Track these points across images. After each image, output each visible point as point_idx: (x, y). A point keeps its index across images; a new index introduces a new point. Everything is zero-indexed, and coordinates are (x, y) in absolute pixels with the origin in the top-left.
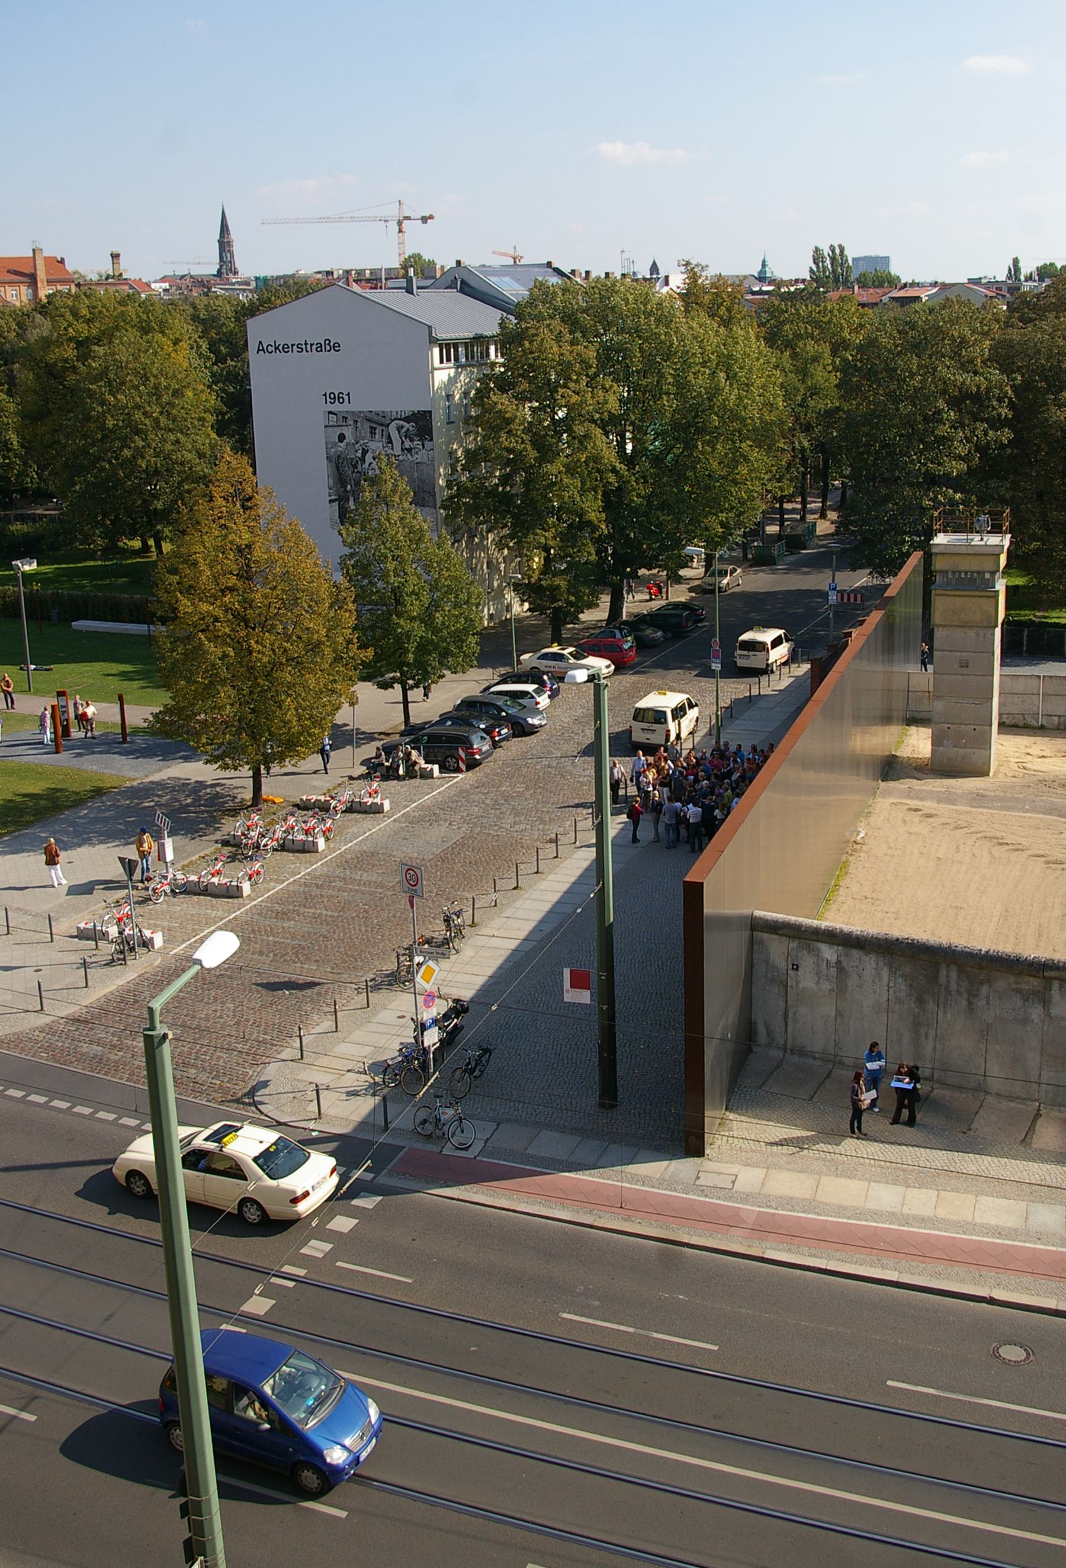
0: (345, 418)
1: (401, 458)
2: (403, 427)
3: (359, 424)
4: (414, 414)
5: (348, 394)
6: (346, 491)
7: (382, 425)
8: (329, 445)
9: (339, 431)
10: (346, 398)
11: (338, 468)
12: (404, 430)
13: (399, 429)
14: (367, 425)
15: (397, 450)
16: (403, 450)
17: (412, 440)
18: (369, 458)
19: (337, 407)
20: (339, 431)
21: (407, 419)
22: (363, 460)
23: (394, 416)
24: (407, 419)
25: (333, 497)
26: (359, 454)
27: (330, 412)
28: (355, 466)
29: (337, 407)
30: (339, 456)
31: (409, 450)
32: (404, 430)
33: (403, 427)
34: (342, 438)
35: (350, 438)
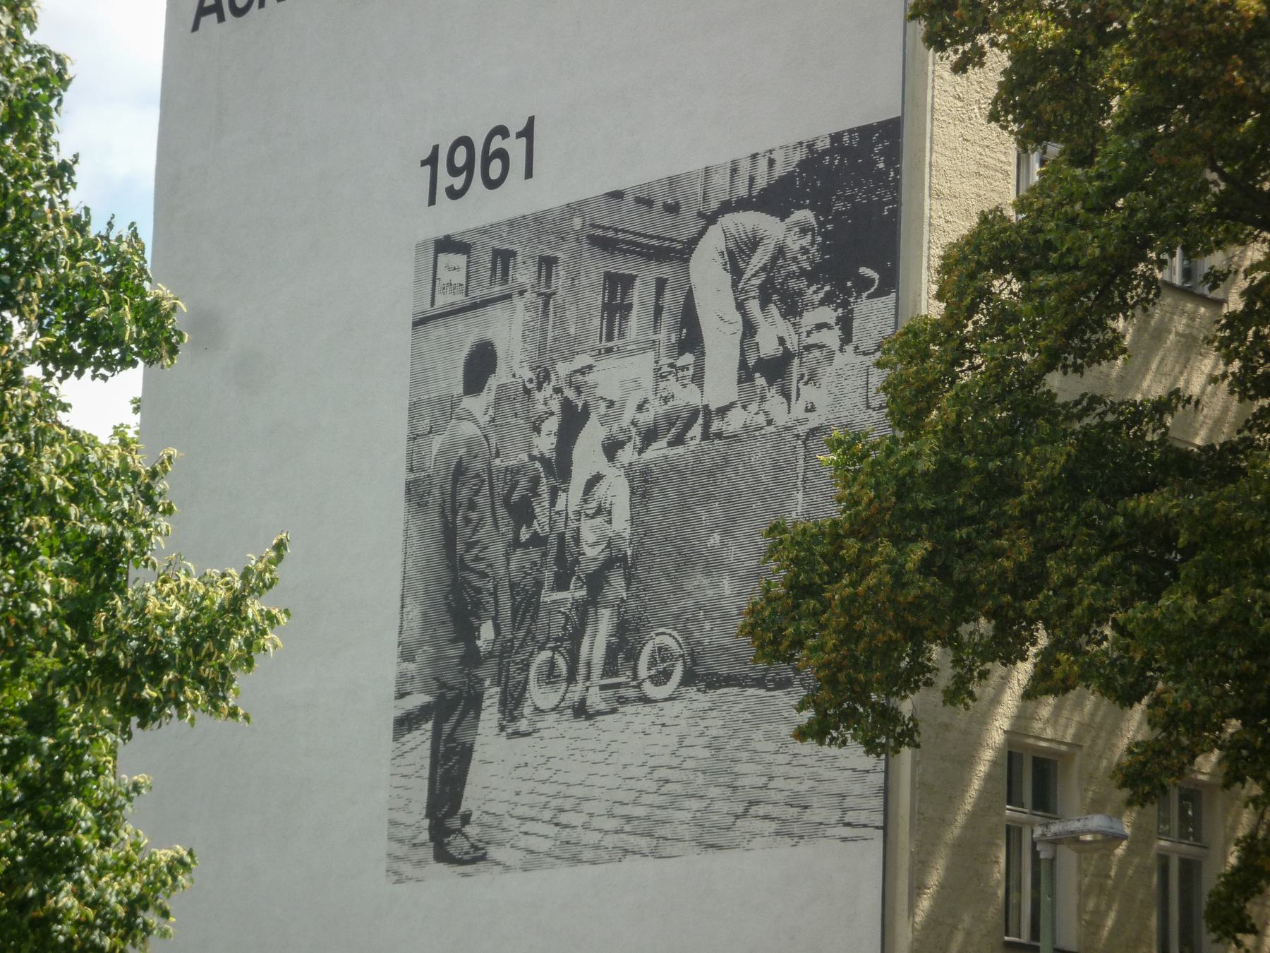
0: (503, 259)
1: (735, 421)
2: (754, 243)
3: (561, 275)
4: (813, 161)
5: (528, 132)
6: (472, 658)
7: (660, 254)
8: (427, 414)
9: (466, 333)
10: (515, 148)
11: (449, 534)
12: (759, 259)
13: (735, 260)
14: (596, 267)
15: (721, 383)
16: (745, 374)
17: (792, 310)
18: (587, 454)
19: (480, 210)
20: (466, 333)
21: (775, 199)
22: (560, 466)
23: (721, 187)
24: (775, 199)
25: (418, 700)
26: (546, 443)
27: (446, 245)
28: (522, 512)
29: (480, 210)
30: (460, 471)
31: (776, 369)
32: (759, 259)
33: (754, 243)
34: (481, 364)
35: (513, 366)
